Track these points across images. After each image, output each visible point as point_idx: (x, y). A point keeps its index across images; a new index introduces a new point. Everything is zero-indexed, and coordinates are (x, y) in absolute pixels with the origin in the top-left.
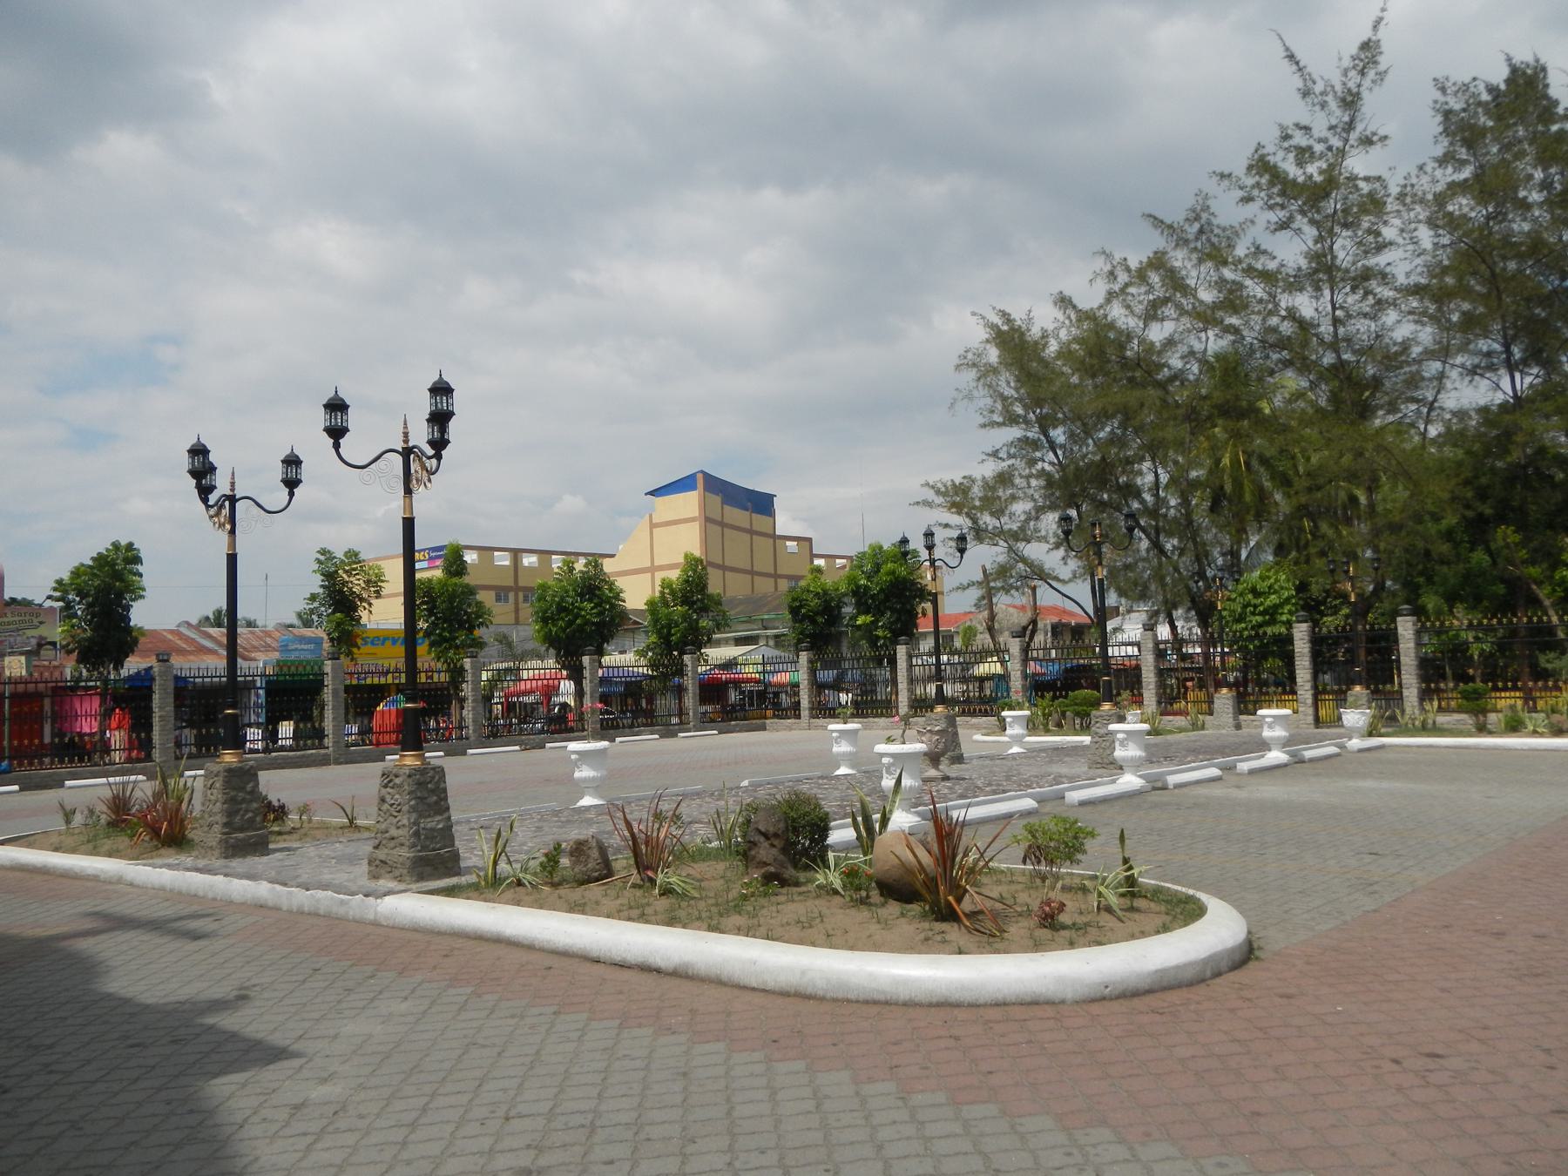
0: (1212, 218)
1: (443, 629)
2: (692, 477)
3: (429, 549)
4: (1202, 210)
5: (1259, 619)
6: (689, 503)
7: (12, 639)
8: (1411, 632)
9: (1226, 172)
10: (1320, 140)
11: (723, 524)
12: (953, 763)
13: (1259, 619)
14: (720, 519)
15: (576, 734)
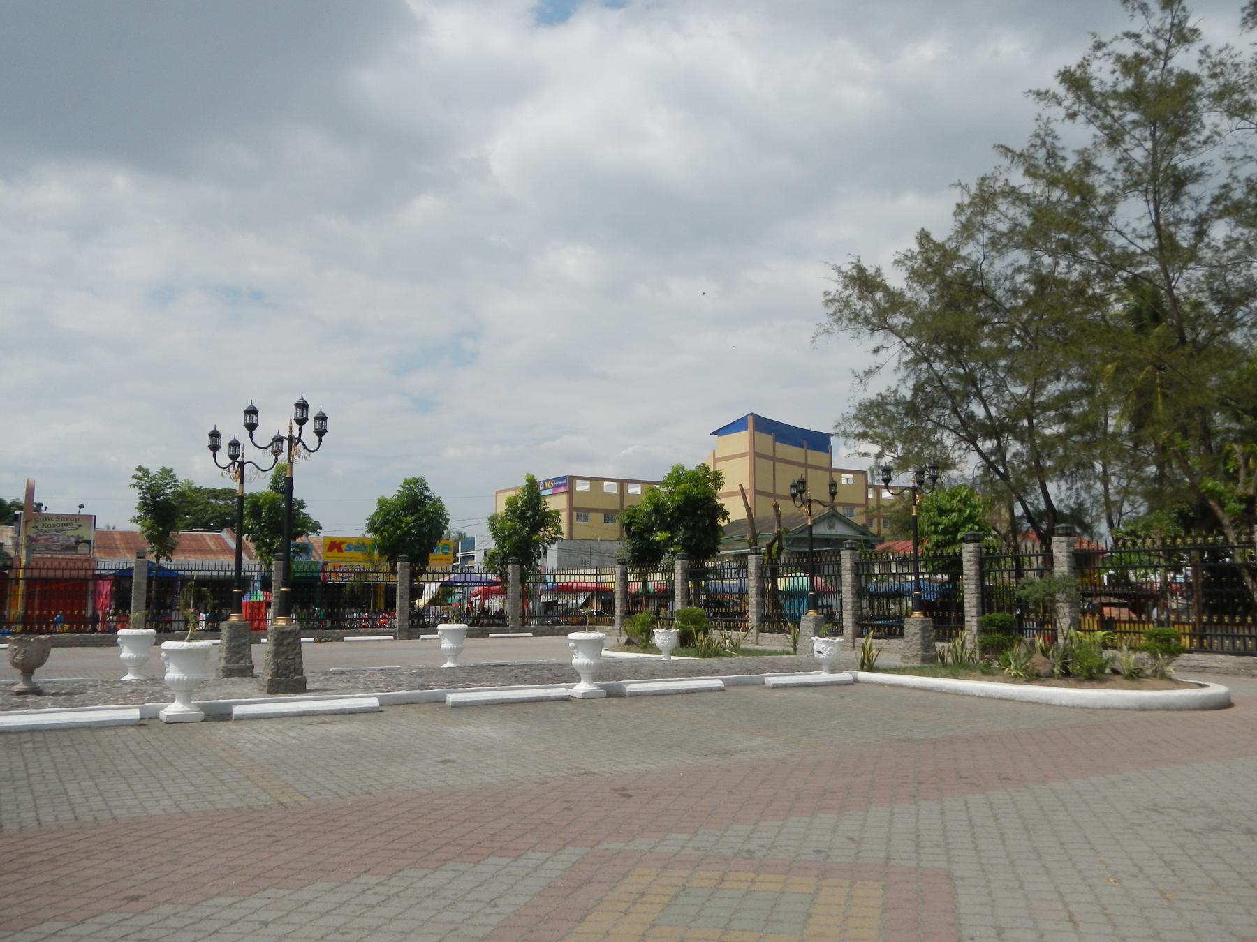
0: (1055, 141)
1: (266, 537)
2: (744, 419)
3: (554, 479)
4: (1047, 135)
5: (940, 538)
6: (741, 441)
7: (56, 538)
8: (1065, 554)
9: (1043, 90)
10: (1148, 46)
11: (774, 459)
12: (229, 676)
13: (940, 538)
14: (772, 455)
15: (379, 630)
